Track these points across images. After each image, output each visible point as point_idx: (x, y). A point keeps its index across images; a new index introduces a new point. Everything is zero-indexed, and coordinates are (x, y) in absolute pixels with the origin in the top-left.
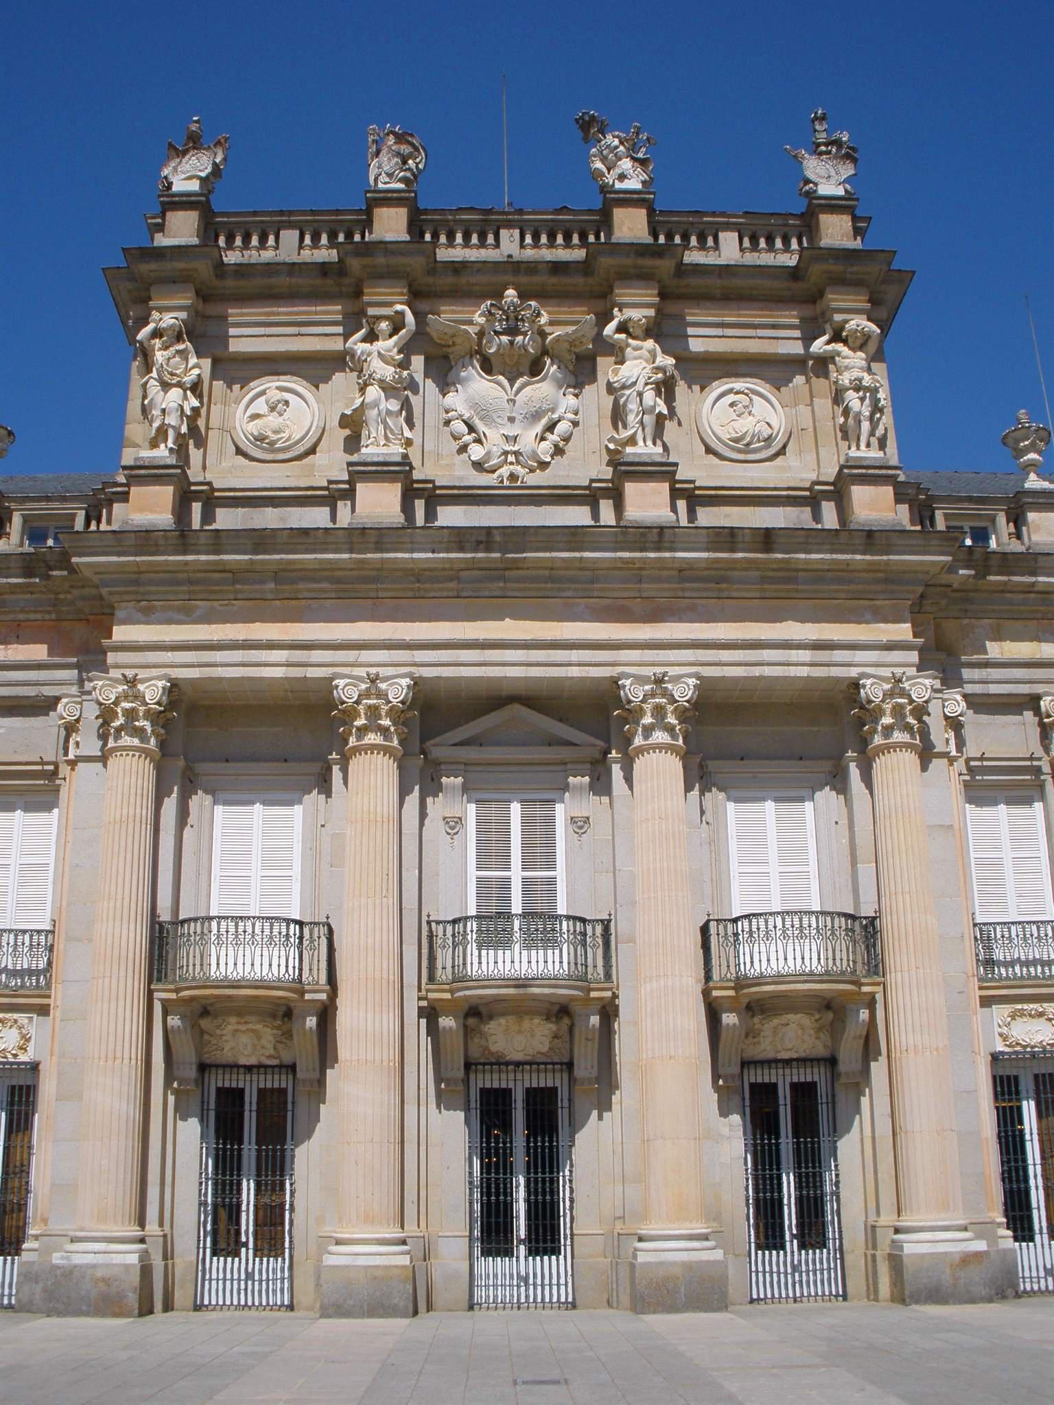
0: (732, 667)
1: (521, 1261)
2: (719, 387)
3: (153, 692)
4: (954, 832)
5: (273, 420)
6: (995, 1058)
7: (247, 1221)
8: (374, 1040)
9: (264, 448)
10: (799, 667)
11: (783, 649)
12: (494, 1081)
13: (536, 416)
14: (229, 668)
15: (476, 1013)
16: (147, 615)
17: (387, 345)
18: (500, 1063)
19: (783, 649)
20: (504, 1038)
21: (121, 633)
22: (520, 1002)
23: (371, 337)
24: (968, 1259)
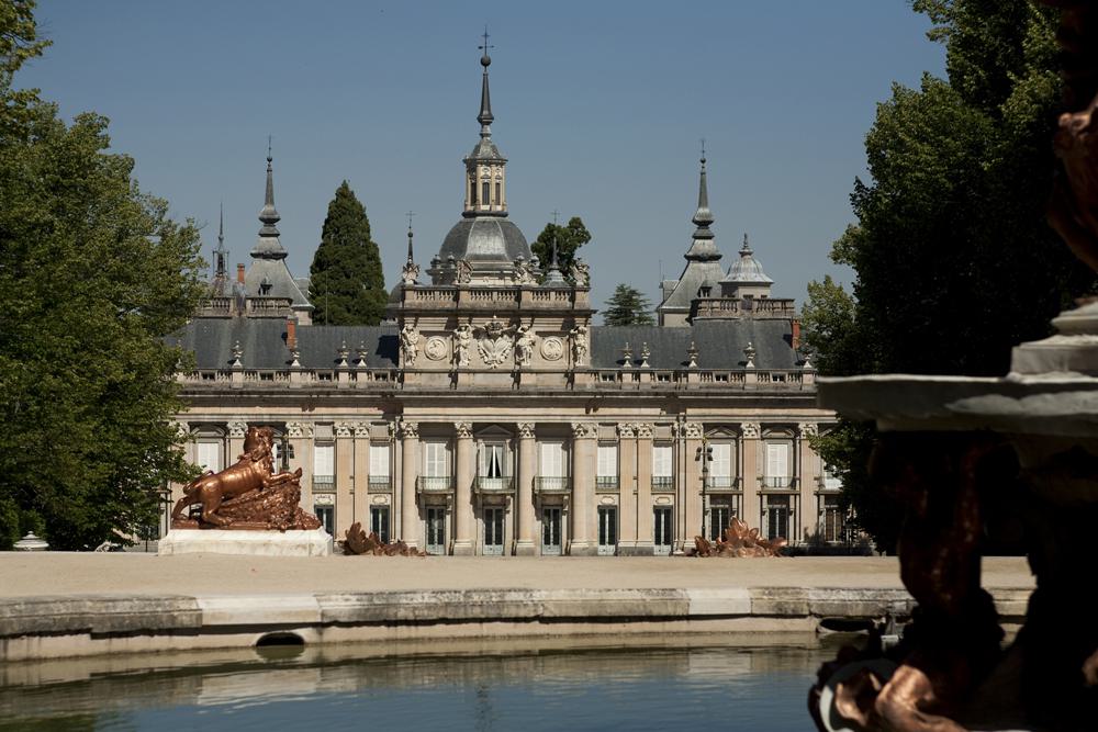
0: (543, 420)
1: (494, 546)
2: (547, 339)
3: (415, 427)
4: (593, 457)
5: (435, 349)
6: (599, 506)
7: (436, 537)
8: (465, 497)
9: (430, 357)
10: (558, 420)
11: (555, 414)
12: (489, 508)
13: (500, 350)
14: (431, 419)
15: (485, 495)
16: (411, 406)
17: (463, 334)
18: (490, 504)
19: (555, 414)
20: (491, 500)
21: (407, 410)
22: (494, 494)
23: (460, 330)
24: (584, 549)
